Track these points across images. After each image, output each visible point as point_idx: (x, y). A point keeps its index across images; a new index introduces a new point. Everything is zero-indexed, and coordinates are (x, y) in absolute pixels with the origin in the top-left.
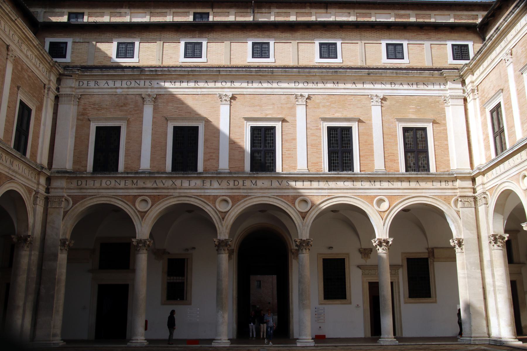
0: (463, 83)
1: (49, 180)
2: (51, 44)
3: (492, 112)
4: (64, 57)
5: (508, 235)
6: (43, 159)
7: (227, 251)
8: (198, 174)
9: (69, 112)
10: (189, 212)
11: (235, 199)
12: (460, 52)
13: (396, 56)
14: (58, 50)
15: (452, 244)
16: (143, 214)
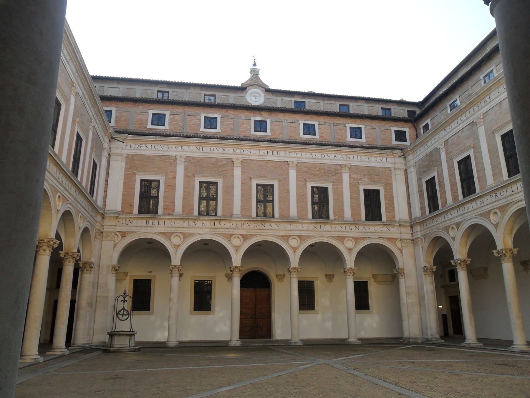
0: (405, 158)
1: (103, 218)
3: (427, 182)
5: (435, 267)
8: (218, 217)
11: (245, 237)
12: (400, 136)
13: (356, 135)
15: (395, 272)
16: (177, 247)
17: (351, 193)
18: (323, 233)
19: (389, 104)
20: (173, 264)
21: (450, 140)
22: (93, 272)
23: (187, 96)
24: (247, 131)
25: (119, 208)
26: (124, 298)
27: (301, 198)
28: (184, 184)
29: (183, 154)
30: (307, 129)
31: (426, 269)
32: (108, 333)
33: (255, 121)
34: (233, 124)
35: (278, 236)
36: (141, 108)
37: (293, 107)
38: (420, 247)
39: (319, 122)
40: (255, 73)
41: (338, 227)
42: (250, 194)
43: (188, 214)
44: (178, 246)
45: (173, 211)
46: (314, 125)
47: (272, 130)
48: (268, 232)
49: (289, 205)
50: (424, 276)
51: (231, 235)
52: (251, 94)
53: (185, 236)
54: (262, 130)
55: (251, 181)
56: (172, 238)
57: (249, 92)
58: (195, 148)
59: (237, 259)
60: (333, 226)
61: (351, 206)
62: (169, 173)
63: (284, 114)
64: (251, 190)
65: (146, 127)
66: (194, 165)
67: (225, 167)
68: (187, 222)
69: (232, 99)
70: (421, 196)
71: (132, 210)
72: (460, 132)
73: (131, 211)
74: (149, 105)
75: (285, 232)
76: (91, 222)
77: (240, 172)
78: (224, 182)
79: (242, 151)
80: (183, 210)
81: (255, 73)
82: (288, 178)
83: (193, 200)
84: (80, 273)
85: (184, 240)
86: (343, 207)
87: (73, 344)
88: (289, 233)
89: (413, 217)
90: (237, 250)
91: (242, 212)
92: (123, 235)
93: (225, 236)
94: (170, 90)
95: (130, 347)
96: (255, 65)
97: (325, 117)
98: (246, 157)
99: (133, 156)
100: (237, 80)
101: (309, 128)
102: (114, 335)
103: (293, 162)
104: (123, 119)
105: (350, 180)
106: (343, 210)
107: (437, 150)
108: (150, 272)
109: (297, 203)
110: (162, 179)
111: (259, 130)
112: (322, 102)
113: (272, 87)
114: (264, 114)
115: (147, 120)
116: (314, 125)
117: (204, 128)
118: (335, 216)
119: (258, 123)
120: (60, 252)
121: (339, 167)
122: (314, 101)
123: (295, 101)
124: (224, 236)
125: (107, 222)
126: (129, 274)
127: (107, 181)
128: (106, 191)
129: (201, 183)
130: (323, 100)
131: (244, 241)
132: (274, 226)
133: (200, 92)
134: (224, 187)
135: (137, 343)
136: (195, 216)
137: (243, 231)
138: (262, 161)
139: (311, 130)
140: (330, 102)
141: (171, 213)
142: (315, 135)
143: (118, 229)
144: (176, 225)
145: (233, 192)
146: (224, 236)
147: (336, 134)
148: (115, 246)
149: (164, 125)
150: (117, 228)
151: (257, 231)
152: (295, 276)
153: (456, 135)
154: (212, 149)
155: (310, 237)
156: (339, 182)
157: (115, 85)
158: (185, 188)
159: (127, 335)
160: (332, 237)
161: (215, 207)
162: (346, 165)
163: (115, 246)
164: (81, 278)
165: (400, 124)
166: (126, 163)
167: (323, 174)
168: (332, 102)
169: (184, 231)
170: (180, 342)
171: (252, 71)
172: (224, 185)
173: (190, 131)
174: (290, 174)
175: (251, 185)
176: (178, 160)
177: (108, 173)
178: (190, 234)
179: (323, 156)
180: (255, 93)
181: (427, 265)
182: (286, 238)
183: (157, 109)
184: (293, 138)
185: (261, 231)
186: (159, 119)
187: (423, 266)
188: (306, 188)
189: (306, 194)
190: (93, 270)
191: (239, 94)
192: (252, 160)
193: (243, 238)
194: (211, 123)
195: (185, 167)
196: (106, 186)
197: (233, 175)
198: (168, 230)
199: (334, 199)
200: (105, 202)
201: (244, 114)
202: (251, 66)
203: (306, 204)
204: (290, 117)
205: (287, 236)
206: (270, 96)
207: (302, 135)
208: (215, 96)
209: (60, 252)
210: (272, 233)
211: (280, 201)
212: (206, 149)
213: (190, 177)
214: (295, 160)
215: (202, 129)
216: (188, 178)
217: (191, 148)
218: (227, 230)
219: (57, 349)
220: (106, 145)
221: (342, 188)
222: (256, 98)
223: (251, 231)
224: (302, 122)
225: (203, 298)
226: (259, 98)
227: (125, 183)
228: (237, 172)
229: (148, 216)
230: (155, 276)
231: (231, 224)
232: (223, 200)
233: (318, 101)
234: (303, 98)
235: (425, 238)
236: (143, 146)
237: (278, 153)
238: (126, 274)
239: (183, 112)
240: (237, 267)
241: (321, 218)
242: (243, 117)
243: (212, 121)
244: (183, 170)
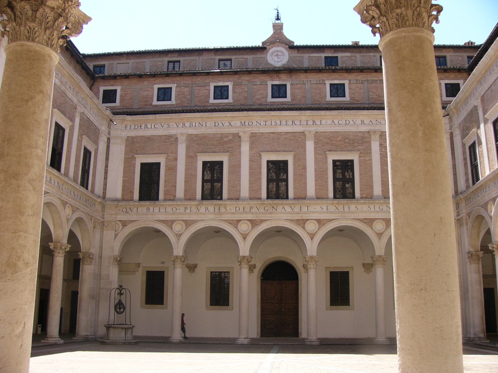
0: (451, 120)
2: (105, 91)
4: (115, 101)
5: (482, 252)
6: (99, 189)
7: (247, 266)
10: (218, 232)
11: (254, 223)
14: (109, 96)
16: (179, 236)
17: (381, 165)
18: (347, 215)
19: (444, 50)
20: (175, 254)
21: (485, 96)
23: (198, 63)
24: (263, 98)
25: (119, 195)
26: (121, 291)
27: (320, 175)
28: (186, 165)
29: (185, 131)
30: (334, 91)
31: (469, 255)
32: (105, 326)
33: (273, 85)
34: (247, 92)
35: (292, 221)
36: (146, 83)
37: (323, 65)
38: (465, 227)
39: (350, 81)
40: (278, 28)
41: (365, 208)
42: (260, 173)
43: (190, 200)
45: (175, 196)
46: (344, 85)
47: (292, 95)
48: (281, 215)
49: (305, 183)
50: (468, 265)
51: (239, 221)
52: (272, 53)
53: (188, 223)
54: (281, 96)
55: (261, 158)
56: (173, 226)
57: (270, 51)
58: (197, 124)
59: (244, 249)
60: (359, 207)
61: (382, 181)
62: (169, 154)
63: (307, 74)
64: (260, 168)
65: (151, 104)
66: (197, 143)
67: (230, 143)
68: (189, 208)
69: (250, 61)
70: (466, 164)
71: (133, 197)
72: (493, 86)
73: (132, 200)
74: (154, 79)
75: (300, 215)
76: (85, 211)
77: (248, 148)
78: (230, 161)
79: (250, 123)
80: (185, 194)
81: (278, 28)
82: (305, 151)
83: (196, 183)
84: (81, 263)
85: (186, 229)
86: (372, 182)
87: (78, 335)
88: (305, 217)
89: (459, 191)
90: (244, 238)
91: (250, 194)
92: (124, 224)
93: (230, 222)
94: (181, 59)
95: (126, 340)
96: (278, 19)
97: (357, 74)
98: (255, 130)
99: (133, 138)
100: (256, 40)
101: (337, 89)
102: (110, 327)
103: (310, 132)
104: (127, 98)
105: (380, 149)
106: (372, 187)
107: (475, 108)
108: (163, 263)
109: (316, 180)
111: (278, 96)
112: (358, 55)
113: (298, 42)
114: (283, 76)
115: (153, 96)
116: (344, 85)
117: (214, 99)
118: (361, 194)
119: (275, 87)
120: (50, 244)
121: (367, 135)
122: (348, 54)
123: (325, 57)
124: (230, 222)
126: (141, 265)
127: (107, 166)
128: (106, 178)
129: (205, 163)
130: (360, 52)
131: (253, 227)
132: (288, 209)
133: (214, 57)
134: (230, 166)
135: (135, 337)
136: (198, 201)
137: (252, 216)
138: (273, 133)
139: (340, 91)
140: (368, 54)
141: (172, 198)
142: (344, 96)
144: (178, 211)
145: (240, 171)
146: (230, 222)
147: (371, 93)
148: (116, 236)
149: (170, 100)
151: (268, 215)
152: (312, 266)
153: (490, 90)
154: (217, 124)
155: (331, 220)
156: (367, 152)
157: (124, 60)
158: (187, 170)
159: (122, 328)
160: (358, 219)
161: (220, 190)
162: (375, 132)
163: (116, 236)
164: (82, 268)
165: (452, 75)
166: (126, 147)
167: (348, 145)
168: (372, 54)
169: (186, 218)
171: (274, 26)
172: (229, 165)
173: (198, 104)
174: (307, 146)
175: (261, 162)
176: (179, 139)
177: (107, 159)
178: (193, 221)
179: (348, 122)
180: (277, 51)
181: (472, 250)
182: (302, 223)
183: (163, 83)
184: (318, 102)
185: (272, 215)
186: (165, 94)
187: (467, 251)
188: (326, 162)
189: (327, 169)
190: (93, 261)
191: (259, 55)
192: (262, 133)
193: (251, 224)
194: (221, 92)
195: (187, 146)
196: (106, 172)
197: (240, 152)
198: (169, 218)
199: (361, 174)
200: (105, 189)
201: (258, 79)
202: (274, 21)
203: (327, 182)
204: (314, 78)
205: (303, 219)
206: (295, 54)
207: (328, 98)
208: (231, 60)
209: (50, 244)
210: (285, 216)
211: (295, 179)
212: (210, 123)
213: (192, 157)
214: (313, 129)
215: (212, 101)
216: (191, 158)
217: (194, 124)
218: (233, 215)
219: (51, 338)
220: (103, 128)
221: (371, 160)
222: (278, 58)
223: (260, 215)
224: (328, 83)
225: (220, 291)
226: (282, 57)
227: (125, 167)
228: (245, 148)
229: (148, 203)
230: (168, 268)
231: (238, 209)
232: (229, 181)
233: (353, 54)
234: (335, 52)
235: (469, 217)
236: (143, 126)
237: (293, 122)
238: (138, 265)
239: (191, 82)
240: (244, 257)
241: (344, 197)
242: (258, 83)
243: (223, 91)
244: (185, 150)
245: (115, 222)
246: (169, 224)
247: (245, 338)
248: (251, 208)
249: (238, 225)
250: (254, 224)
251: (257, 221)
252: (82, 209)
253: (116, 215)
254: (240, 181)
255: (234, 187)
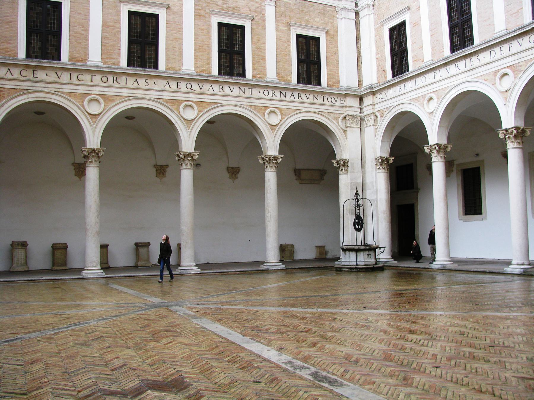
9: (368, 22)
22: (349, 171)
44: (433, 112)
93: (486, 78)
95: (357, 265)
110: (406, 17)
125: (367, 101)
126: (456, 163)
143: (378, 107)
150: (376, 106)
170: (455, 261)
193: (514, 72)
230: (483, 161)
245: (374, 114)
246: (421, 101)
247: (518, 264)
248: (511, 45)
249: (495, 80)
250: (516, 72)
251: (521, 66)
252: (307, 110)
253: (374, 105)
254: (492, 8)
255: (485, 20)
